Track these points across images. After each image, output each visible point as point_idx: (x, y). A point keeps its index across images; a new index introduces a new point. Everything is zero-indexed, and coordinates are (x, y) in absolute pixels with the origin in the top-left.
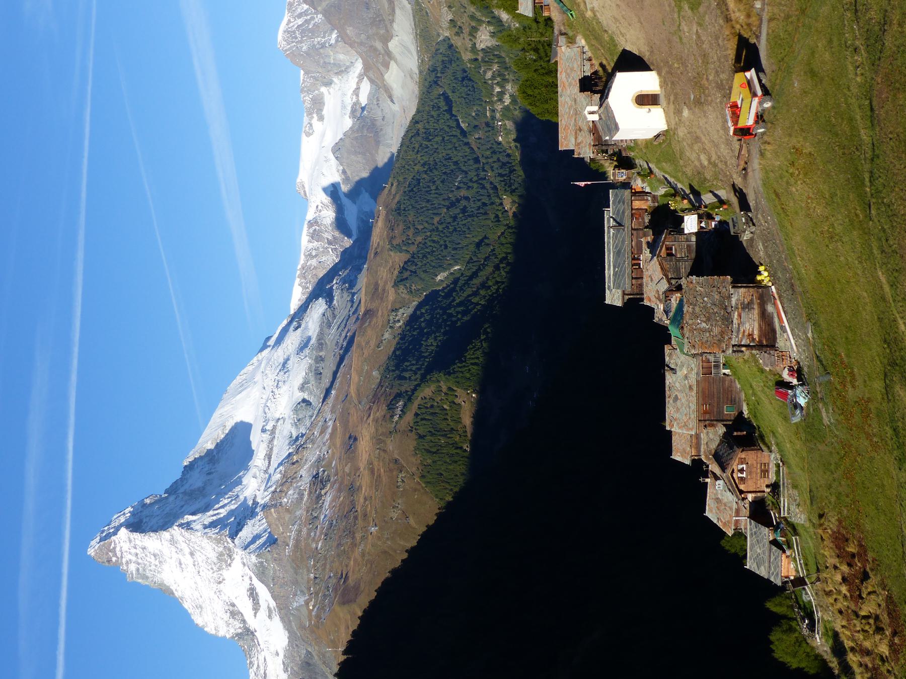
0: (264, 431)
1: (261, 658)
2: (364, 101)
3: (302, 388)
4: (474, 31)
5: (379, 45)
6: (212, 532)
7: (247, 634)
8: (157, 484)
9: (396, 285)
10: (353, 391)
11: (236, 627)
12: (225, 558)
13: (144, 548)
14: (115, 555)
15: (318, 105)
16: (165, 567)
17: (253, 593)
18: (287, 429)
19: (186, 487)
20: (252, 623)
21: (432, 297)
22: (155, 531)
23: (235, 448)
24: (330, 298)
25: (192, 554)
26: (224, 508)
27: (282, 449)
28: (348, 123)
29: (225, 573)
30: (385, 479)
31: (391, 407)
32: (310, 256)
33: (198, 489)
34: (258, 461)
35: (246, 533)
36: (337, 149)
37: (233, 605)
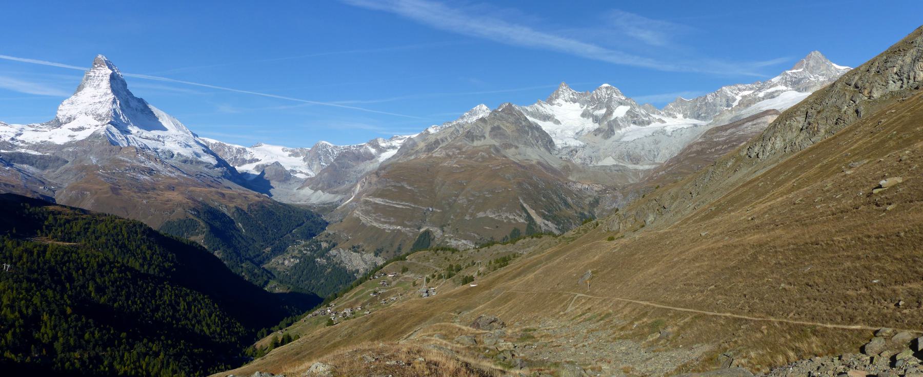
2: (298, 175)
3: (178, 154)
4: (327, 242)
5: (320, 185)
6: (111, 113)
7: (58, 124)
8: (136, 90)
9: (236, 207)
10: (192, 188)
12: (99, 117)
15: (296, 154)
17: (81, 129)
18: (160, 147)
20: (65, 127)
21: (232, 222)
23: (149, 120)
24: (217, 166)
27: (151, 144)
28: (288, 169)
29: (91, 116)
30: (166, 207)
31: (194, 209)
32: (229, 148)
33: (132, 108)
34: (146, 133)
35: (114, 130)
36: (277, 163)
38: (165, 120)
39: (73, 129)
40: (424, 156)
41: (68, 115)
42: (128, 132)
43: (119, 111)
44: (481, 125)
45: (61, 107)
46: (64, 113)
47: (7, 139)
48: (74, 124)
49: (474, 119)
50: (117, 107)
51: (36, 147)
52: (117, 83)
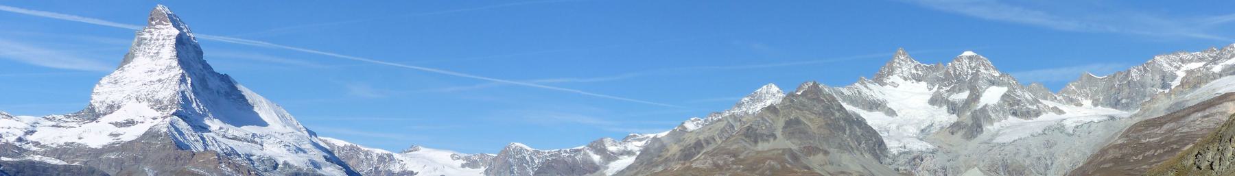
0: (254, 135)
1: (73, 124)
6: (178, 98)
8: (218, 61)
12: (158, 105)
16: (149, 60)
17: (130, 123)
18: (256, 152)
23: (235, 107)
25: (160, 81)
27: (242, 148)
29: (145, 104)
33: (211, 90)
34: (233, 130)
35: (182, 125)
37: (119, 107)
38: (264, 109)
39: (117, 124)
40: (677, 167)
41: (109, 102)
42: (206, 129)
43: (190, 95)
44: (770, 117)
45: (97, 89)
46: (102, 98)
47: (12, 139)
49: (758, 107)
51: (58, 152)
52: (187, 51)
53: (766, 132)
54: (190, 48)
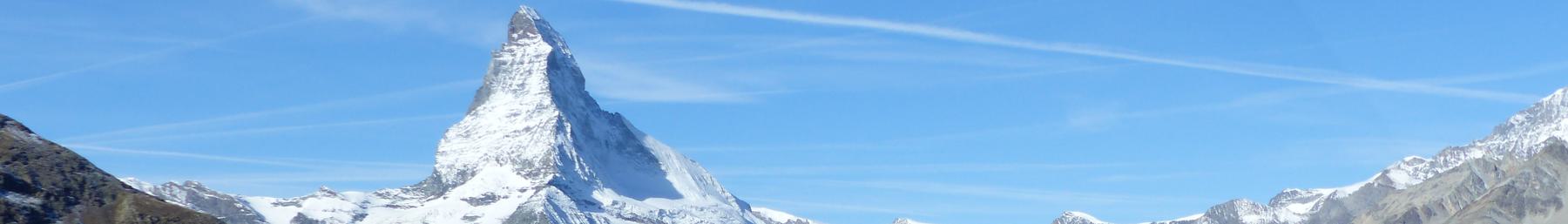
0: (661, 212)
6: (554, 156)
11: (448, 176)
12: (526, 168)
13: (530, 72)
14: (520, 37)
16: (510, 96)
17: (489, 199)
19: (592, 117)
20: (454, 194)
22: (551, 87)
25: (527, 129)
26: (581, 169)
29: (508, 167)
35: (563, 200)
37: (473, 174)
38: (677, 176)
39: (473, 201)
41: (459, 165)
42: (597, 206)
43: (572, 152)
44: (1551, 166)
45: (443, 146)
48: (473, 188)
50: (566, 139)
52: (564, 78)
53: (1542, 196)
54: (567, 74)
